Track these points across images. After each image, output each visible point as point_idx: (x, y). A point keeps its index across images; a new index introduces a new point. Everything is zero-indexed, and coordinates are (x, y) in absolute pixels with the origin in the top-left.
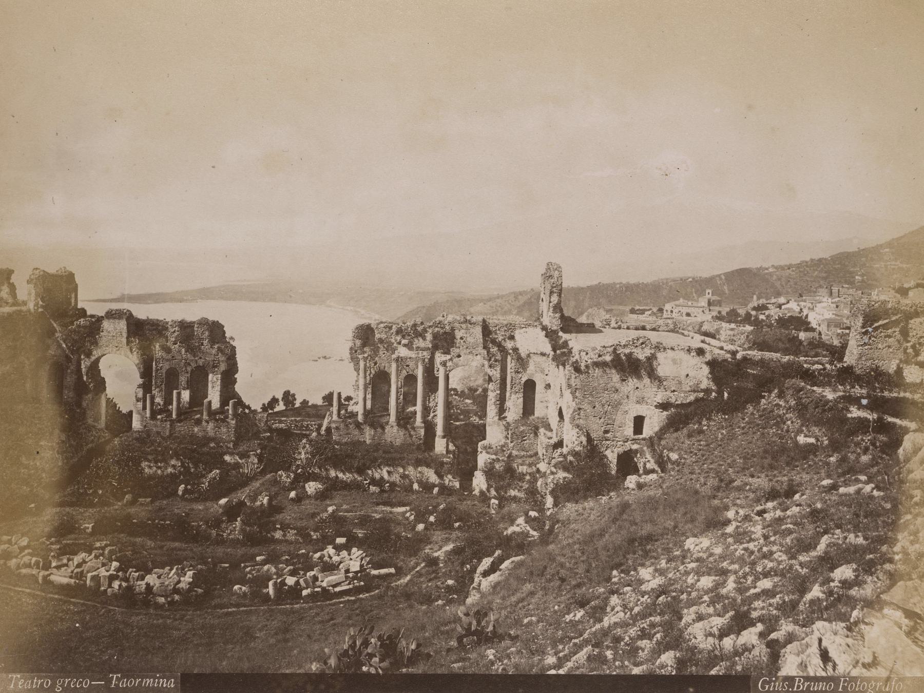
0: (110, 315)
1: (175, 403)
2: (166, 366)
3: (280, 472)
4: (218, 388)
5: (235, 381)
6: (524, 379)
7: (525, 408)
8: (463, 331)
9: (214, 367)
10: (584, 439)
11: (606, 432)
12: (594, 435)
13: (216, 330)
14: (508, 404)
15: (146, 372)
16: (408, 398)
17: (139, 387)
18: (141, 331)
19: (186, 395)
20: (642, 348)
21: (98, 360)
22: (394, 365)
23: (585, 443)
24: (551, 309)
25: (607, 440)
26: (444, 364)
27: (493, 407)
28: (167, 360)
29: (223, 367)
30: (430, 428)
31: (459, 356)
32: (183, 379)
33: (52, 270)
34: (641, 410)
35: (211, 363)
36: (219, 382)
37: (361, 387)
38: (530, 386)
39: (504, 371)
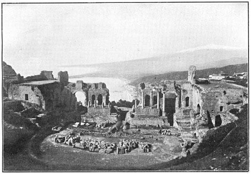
0: (78, 82)
2: (92, 94)
4: (105, 100)
5: (109, 98)
13: (104, 85)
14: (182, 103)
15: (87, 96)
18: (85, 86)
19: (97, 102)
21: (75, 93)
22: (151, 93)
26: (164, 93)
29: (106, 94)
32: (96, 98)
33: (63, 71)
34: (223, 105)
37: (142, 99)
38: (187, 99)
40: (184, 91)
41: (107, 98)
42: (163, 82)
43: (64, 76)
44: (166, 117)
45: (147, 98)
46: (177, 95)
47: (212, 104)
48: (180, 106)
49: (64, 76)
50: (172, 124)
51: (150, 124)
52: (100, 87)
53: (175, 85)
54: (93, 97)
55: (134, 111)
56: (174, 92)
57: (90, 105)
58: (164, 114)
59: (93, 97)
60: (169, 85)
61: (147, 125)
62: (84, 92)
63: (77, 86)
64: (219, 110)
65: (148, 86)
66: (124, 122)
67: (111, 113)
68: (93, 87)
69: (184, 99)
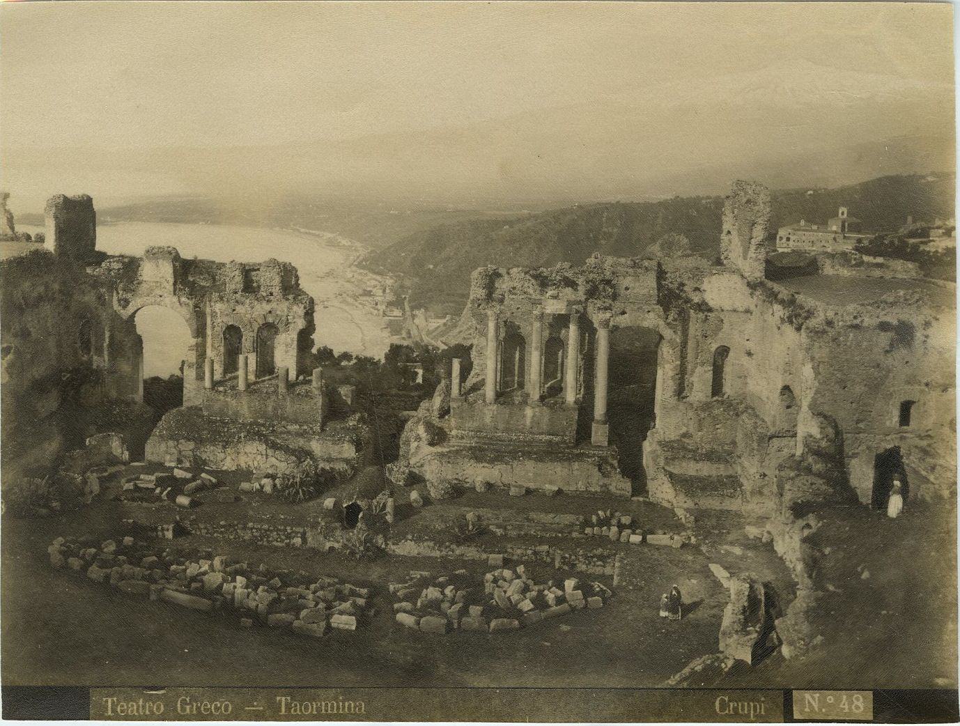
4: (293, 352)
7: (713, 387)
8: (629, 278)
10: (830, 431)
12: (843, 425)
15: (200, 332)
18: (191, 276)
19: (252, 359)
20: (919, 307)
21: (133, 315)
23: (832, 436)
24: (753, 248)
27: (671, 383)
29: (301, 324)
30: (585, 407)
31: (623, 313)
32: (247, 340)
36: (295, 343)
41: (305, 339)
42: (599, 268)
43: (77, 217)
46: (667, 333)
47: (859, 389)
48: (680, 391)
49: (77, 217)
50: (640, 486)
51: (532, 486)
52: (269, 280)
55: (444, 412)
56: (652, 319)
57: (217, 377)
58: (599, 434)
59: (232, 333)
60: (627, 282)
61: (513, 491)
63: (148, 272)
64: (896, 419)
66: (396, 473)
68: (234, 281)
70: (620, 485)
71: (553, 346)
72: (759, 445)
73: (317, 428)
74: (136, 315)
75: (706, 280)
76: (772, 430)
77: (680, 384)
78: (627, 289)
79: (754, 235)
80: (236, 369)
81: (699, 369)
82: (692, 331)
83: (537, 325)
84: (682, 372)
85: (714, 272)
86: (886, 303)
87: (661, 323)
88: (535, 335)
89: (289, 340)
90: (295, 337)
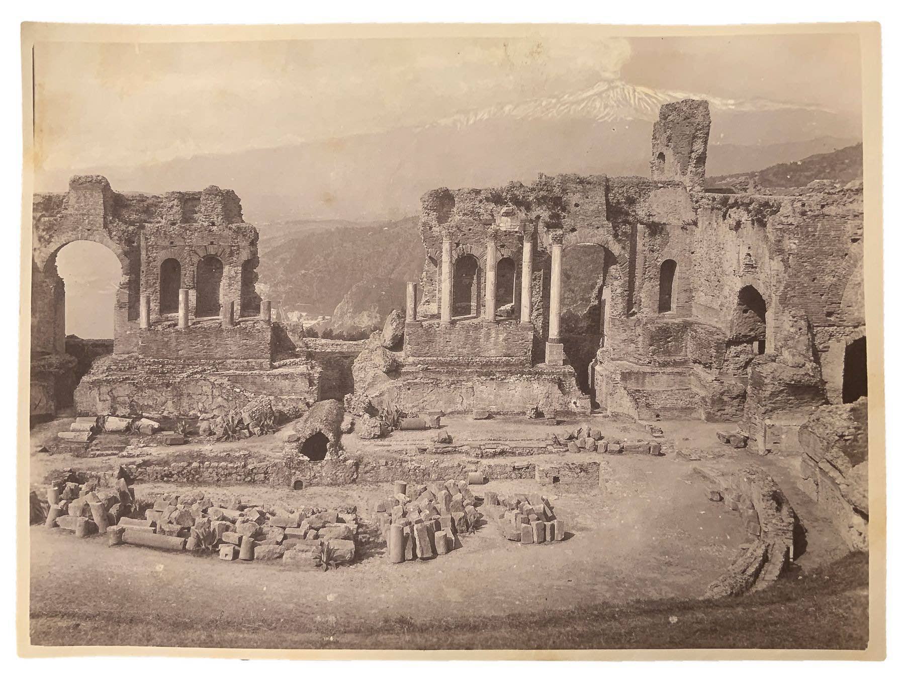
1: (181, 306)
2: (161, 256)
3: (347, 396)
6: (661, 261)
8: (578, 195)
9: (231, 254)
11: (829, 314)
15: (133, 268)
16: (506, 288)
17: (122, 286)
19: (193, 294)
25: (830, 326)
26: (559, 240)
28: (164, 248)
29: (245, 255)
31: (573, 230)
32: (188, 273)
35: (228, 251)
36: (240, 275)
38: (668, 268)
39: (633, 252)
40: (655, 229)
44: (569, 369)
45: (466, 267)
46: (616, 249)
53: (606, 196)
54: (171, 269)
57: (153, 317)
59: (171, 269)
62: (114, 245)
65: (468, 205)
67: (273, 360)
69: (654, 272)
70: (578, 402)
71: (508, 268)
72: (717, 352)
73: (266, 362)
74: (59, 254)
75: (652, 194)
76: (729, 335)
77: (628, 300)
78: (577, 205)
79: (695, 148)
80: (176, 310)
81: (647, 284)
82: (639, 247)
83: (491, 245)
84: (630, 287)
85: (660, 185)
86: (852, 191)
87: (611, 238)
88: (489, 258)
89: (233, 273)
90: (240, 268)
